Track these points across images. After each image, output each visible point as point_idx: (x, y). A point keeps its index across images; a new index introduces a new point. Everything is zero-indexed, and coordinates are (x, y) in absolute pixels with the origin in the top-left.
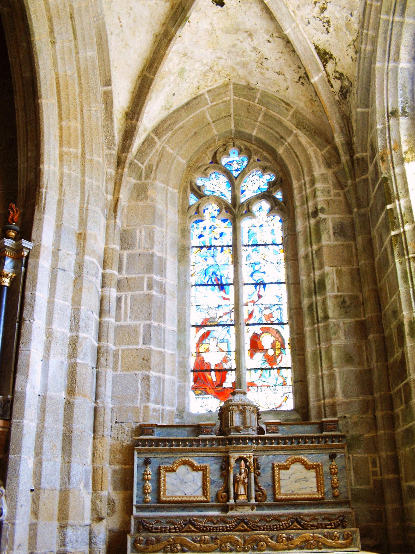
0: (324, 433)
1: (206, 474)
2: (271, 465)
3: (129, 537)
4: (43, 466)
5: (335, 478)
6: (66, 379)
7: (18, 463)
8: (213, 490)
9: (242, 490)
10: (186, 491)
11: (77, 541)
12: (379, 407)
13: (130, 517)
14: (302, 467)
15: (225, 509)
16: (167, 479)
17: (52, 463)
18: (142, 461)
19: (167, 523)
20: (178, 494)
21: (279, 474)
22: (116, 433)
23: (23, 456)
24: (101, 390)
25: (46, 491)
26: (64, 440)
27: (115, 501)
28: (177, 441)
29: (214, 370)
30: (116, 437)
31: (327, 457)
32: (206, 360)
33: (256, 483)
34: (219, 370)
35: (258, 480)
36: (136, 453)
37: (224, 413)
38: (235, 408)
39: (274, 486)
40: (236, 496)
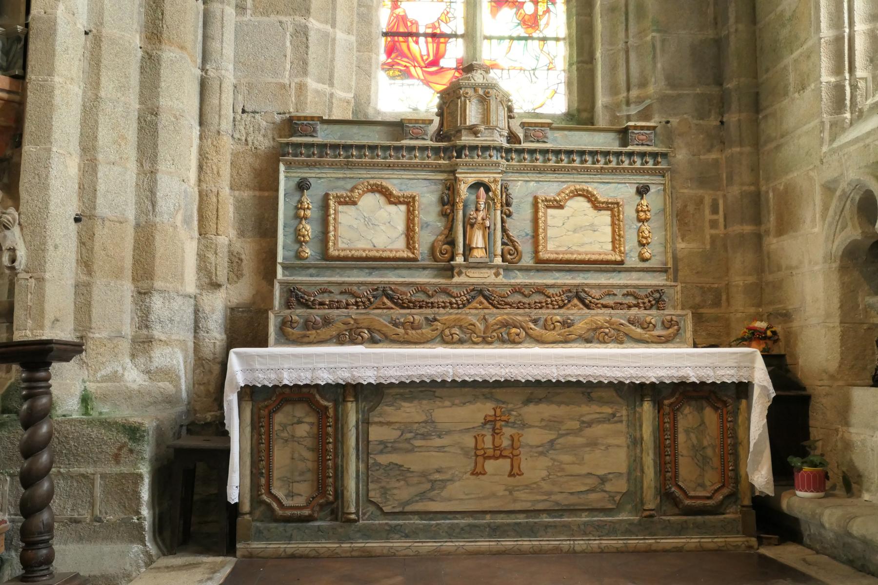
0: (630, 148)
1: (414, 210)
2: (530, 199)
3: (271, 316)
4: (100, 175)
5: (646, 227)
6: (143, 10)
7: (45, 161)
8: (425, 239)
9: (478, 240)
10: (374, 241)
11: (171, 321)
12: (734, 106)
13: (272, 285)
14: (589, 205)
15: (449, 270)
16: (341, 218)
17: (117, 169)
18: (293, 184)
19: (341, 293)
20: (361, 245)
21: (545, 214)
22: (243, 131)
23: (54, 149)
24: (215, 45)
25: (107, 223)
26: (141, 129)
27: (243, 257)
28: (360, 147)
29: (426, 35)
30: (244, 138)
31: (633, 190)
32: (410, 16)
33: (504, 230)
34: (434, 36)
35: (507, 225)
36: (282, 168)
37: (451, 99)
38: (471, 92)
39: (535, 236)
40: (468, 249)
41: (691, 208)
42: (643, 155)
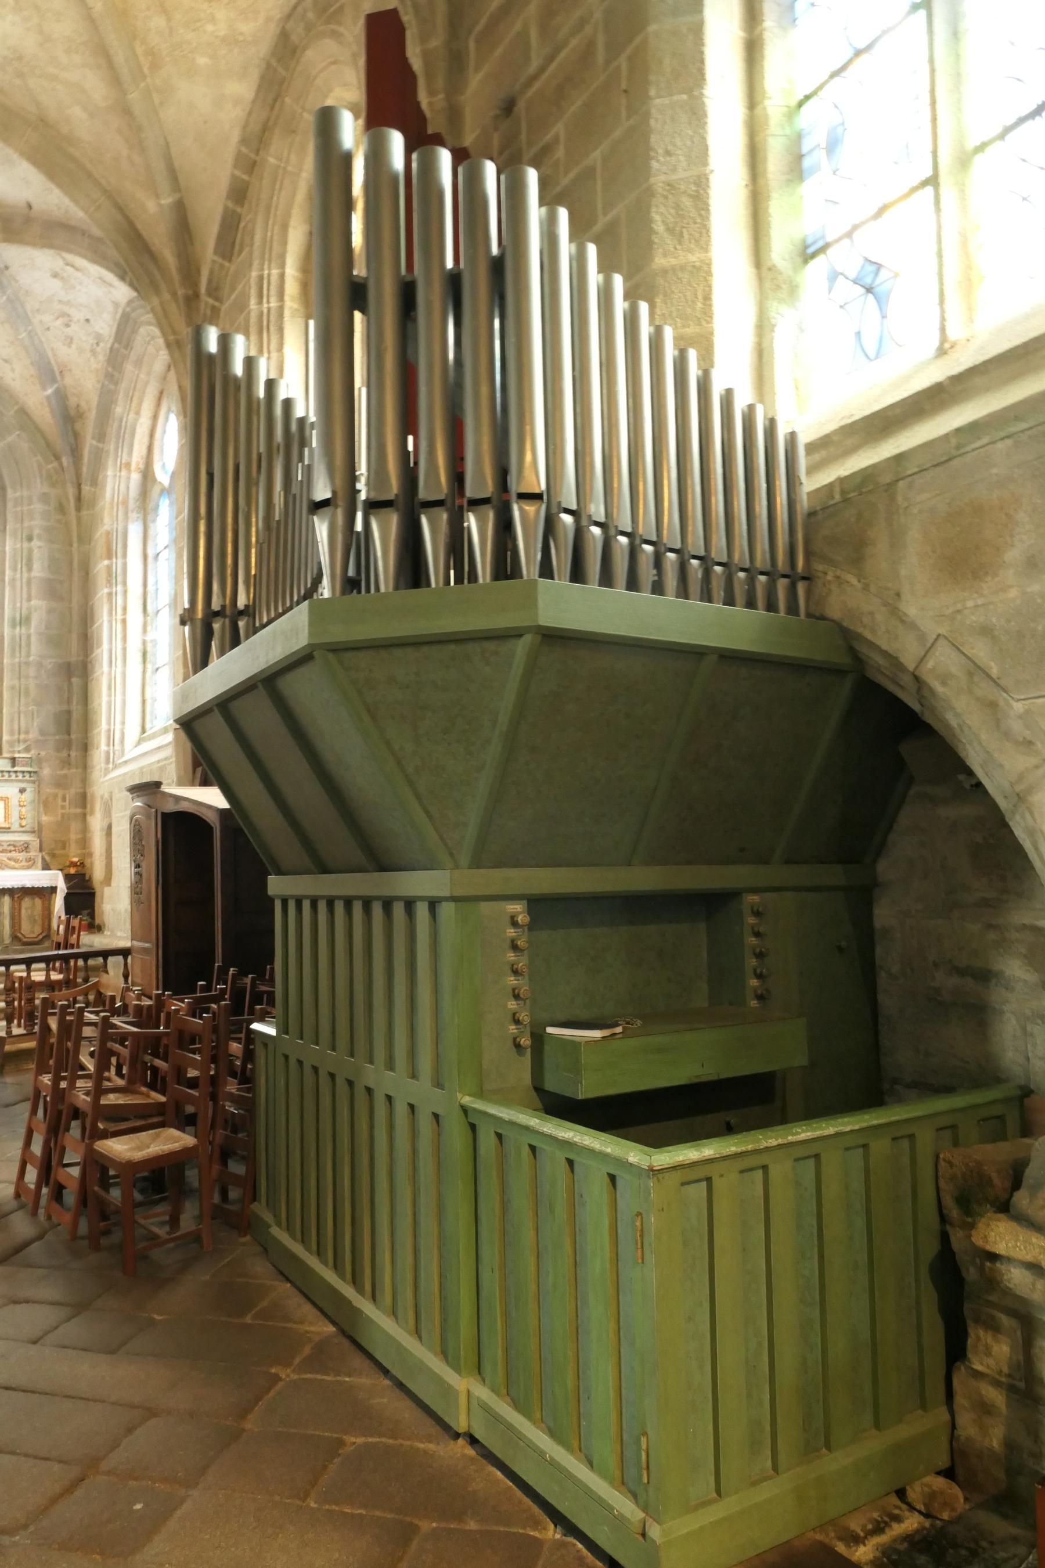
0: (16, 769)
5: (24, 810)
12: (74, 747)
41: (51, 799)
42: (23, 772)
